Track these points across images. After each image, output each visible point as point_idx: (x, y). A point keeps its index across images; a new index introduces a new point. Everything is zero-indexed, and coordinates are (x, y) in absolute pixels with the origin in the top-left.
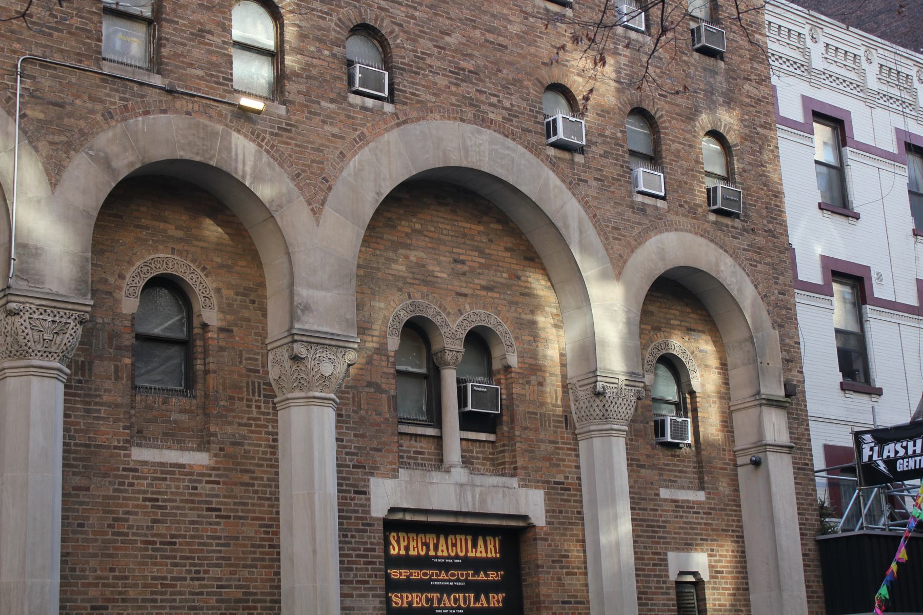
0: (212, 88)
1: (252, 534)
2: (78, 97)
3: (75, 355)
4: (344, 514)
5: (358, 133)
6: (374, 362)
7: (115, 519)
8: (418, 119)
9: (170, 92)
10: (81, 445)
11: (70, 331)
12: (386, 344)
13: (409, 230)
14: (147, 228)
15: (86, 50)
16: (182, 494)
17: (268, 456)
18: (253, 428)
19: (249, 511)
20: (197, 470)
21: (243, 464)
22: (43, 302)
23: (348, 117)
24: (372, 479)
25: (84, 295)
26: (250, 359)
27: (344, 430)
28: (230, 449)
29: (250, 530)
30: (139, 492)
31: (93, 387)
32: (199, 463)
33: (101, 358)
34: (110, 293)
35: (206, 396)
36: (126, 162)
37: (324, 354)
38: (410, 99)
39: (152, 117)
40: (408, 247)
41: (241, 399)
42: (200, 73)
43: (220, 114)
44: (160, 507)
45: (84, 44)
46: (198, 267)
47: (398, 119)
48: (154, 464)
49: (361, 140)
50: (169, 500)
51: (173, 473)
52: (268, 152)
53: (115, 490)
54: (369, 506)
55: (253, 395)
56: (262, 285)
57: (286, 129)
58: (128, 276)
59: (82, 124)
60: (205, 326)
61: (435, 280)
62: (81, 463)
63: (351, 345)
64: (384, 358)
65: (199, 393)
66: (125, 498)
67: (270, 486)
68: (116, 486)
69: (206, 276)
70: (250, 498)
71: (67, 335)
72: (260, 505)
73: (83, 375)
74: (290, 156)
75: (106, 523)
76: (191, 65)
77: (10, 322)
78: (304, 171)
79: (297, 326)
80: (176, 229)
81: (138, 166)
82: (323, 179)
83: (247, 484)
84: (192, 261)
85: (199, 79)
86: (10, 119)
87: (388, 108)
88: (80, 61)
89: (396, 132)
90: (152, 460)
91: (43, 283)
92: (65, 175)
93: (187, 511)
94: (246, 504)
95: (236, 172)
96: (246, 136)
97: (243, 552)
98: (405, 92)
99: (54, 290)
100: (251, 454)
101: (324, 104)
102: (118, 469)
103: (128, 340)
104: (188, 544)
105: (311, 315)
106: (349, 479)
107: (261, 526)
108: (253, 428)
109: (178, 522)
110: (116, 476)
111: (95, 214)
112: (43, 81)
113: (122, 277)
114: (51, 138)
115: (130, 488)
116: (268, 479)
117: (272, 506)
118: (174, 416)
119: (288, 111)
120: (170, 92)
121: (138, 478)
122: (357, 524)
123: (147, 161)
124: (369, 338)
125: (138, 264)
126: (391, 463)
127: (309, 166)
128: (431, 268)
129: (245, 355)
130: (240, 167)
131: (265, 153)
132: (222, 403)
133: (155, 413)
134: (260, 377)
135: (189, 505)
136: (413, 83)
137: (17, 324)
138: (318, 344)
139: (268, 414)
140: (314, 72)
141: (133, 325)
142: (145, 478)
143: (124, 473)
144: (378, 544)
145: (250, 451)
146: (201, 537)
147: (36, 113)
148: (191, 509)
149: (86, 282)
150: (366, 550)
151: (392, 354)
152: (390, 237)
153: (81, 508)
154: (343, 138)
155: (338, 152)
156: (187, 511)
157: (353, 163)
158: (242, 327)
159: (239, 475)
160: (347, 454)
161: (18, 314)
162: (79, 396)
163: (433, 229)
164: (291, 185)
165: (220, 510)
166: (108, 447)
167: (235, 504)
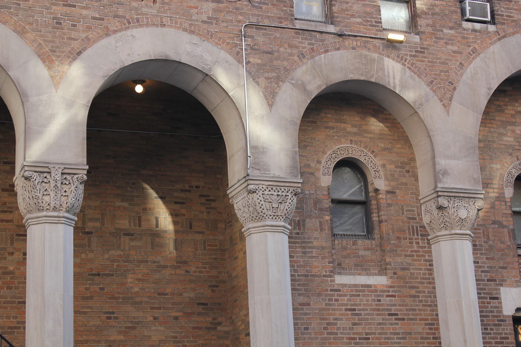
0: (368, 29)
1: (421, 330)
2: (281, 46)
3: (293, 217)
4: (484, 314)
5: (471, 48)
6: (496, 207)
7: (328, 324)
8: (514, 34)
9: (340, 35)
10: (302, 275)
12: (504, 193)
13: (514, 112)
14: (333, 128)
15: (284, 15)
16: (371, 305)
17: (427, 276)
18: (415, 257)
19: (417, 315)
20: (379, 288)
21: (410, 282)
22: (271, 183)
23: (464, 38)
24: (502, 289)
25: (296, 176)
26: (409, 210)
27: (479, 256)
28: (400, 273)
29: (419, 328)
30: (342, 305)
31: (307, 236)
32: (380, 284)
33: (310, 217)
34: (312, 174)
35: (382, 238)
36: (315, 85)
37: (460, 204)
38: (506, 20)
39: (330, 53)
40: (514, 124)
41: (405, 239)
42: (359, 20)
43: (375, 47)
44: (357, 315)
45: (282, 11)
46: (369, 151)
47: (499, 35)
48: (350, 286)
49: (474, 53)
51: (364, 291)
52: (409, 68)
53: (327, 305)
54: (501, 307)
55: (413, 235)
56: (413, 159)
57: (421, 51)
58: (323, 161)
59: (285, 63)
60: (376, 190)
62: (303, 288)
63: (479, 196)
64: (503, 203)
65: (377, 236)
66: (333, 310)
67: (430, 297)
68: (327, 302)
69: (375, 156)
71: (287, 204)
72: (424, 310)
73: (299, 229)
74: (425, 69)
75: (322, 327)
76: (353, 16)
77: (250, 198)
78: (436, 79)
79: (439, 185)
80: (352, 127)
81: (324, 87)
82: (449, 83)
83: (414, 296)
84: (364, 148)
85: (360, 25)
86: (240, 66)
87: (491, 28)
88: (281, 22)
89: (498, 44)
90: (349, 283)
91: (269, 171)
92: (278, 98)
93: (375, 316)
94: (414, 310)
95: (389, 85)
96: (394, 59)
97: (416, 343)
98: (502, 15)
100: (415, 276)
101: (445, 31)
102: (327, 290)
103: (327, 204)
104: (377, 339)
105: (449, 177)
106: (485, 289)
107: (426, 324)
109: (370, 324)
110: (326, 295)
111: (299, 122)
112: (259, 38)
113: (319, 162)
114: (266, 75)
115: (336, 303)
116: (429, 292)
117: (433, 311)
118: (361, 253)
119: (421, 39)
120: (340, 35)
121: (340, 296)
122: (494, 321)
123: (329, 84)
124: (491, 190)
125: (329, 152)
126: (514, 277)
127: (439, 75)
129: (405, 208)
130: (391, 80)
131: (407, 70)
132: (393, 242)
134: (417, 223)
135: (376, 312)
136: (508, 8)
137: (255, 199)
138: (455, 197)
139: (425, 247)
140: (437, 10)
141: (329, 194)
143: (331, 293)
144: (510, 334)
145: (414, 273)
146: (386, 334)
147: (256, 60)
148: (378, 315)
149: (297, 168)
150: (501, 338)
151: (509, 200)
152: (500, 118)
153: (305, 317)
154: (461, 53)
155: (458, 63)
156: (375, 316)
157: (470, 70)
159: (408, 290)
160: (482, 272)
161: (255, 192)
162: (298, 243)
164: (428, 89)
165: (397, 315)
166: (319, 276)
167: (407, 310)
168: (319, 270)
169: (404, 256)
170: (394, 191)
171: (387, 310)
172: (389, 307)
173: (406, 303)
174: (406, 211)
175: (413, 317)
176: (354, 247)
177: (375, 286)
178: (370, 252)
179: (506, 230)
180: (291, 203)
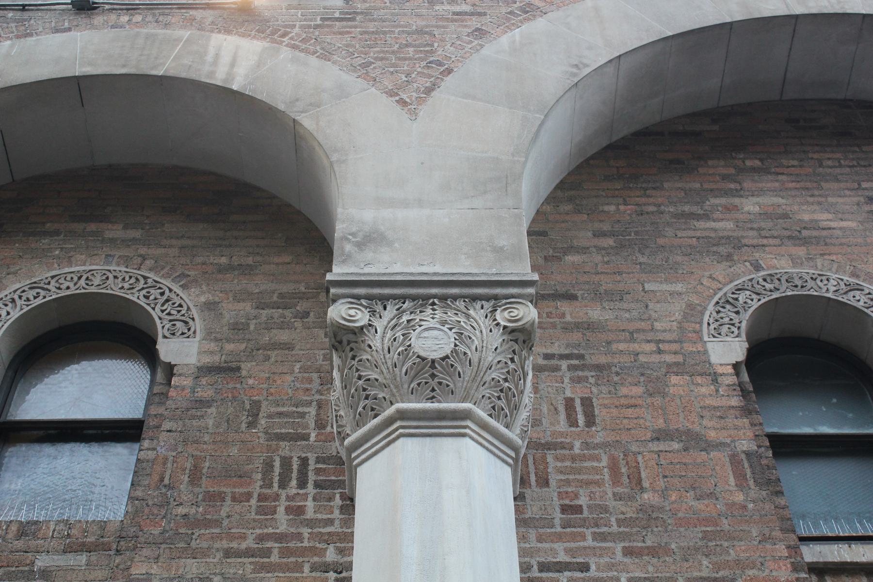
12: (706, 352)
18: (275, 558)
26: (280, 414)
27: (589, 542)
46: (166, 276)
55: (283, 485)
61: (825, 233)
108: (275, 558)
128: (806, 217)
132: (181, 510)
134: (311, 448)
138: (403, 298)
139: (331, 522)
158: (267, 358)
163: (795, 163)
169: (219, 555)
170: (234, 365)
174: (270, 416)
176: (19, 544)
179: (721, 457)
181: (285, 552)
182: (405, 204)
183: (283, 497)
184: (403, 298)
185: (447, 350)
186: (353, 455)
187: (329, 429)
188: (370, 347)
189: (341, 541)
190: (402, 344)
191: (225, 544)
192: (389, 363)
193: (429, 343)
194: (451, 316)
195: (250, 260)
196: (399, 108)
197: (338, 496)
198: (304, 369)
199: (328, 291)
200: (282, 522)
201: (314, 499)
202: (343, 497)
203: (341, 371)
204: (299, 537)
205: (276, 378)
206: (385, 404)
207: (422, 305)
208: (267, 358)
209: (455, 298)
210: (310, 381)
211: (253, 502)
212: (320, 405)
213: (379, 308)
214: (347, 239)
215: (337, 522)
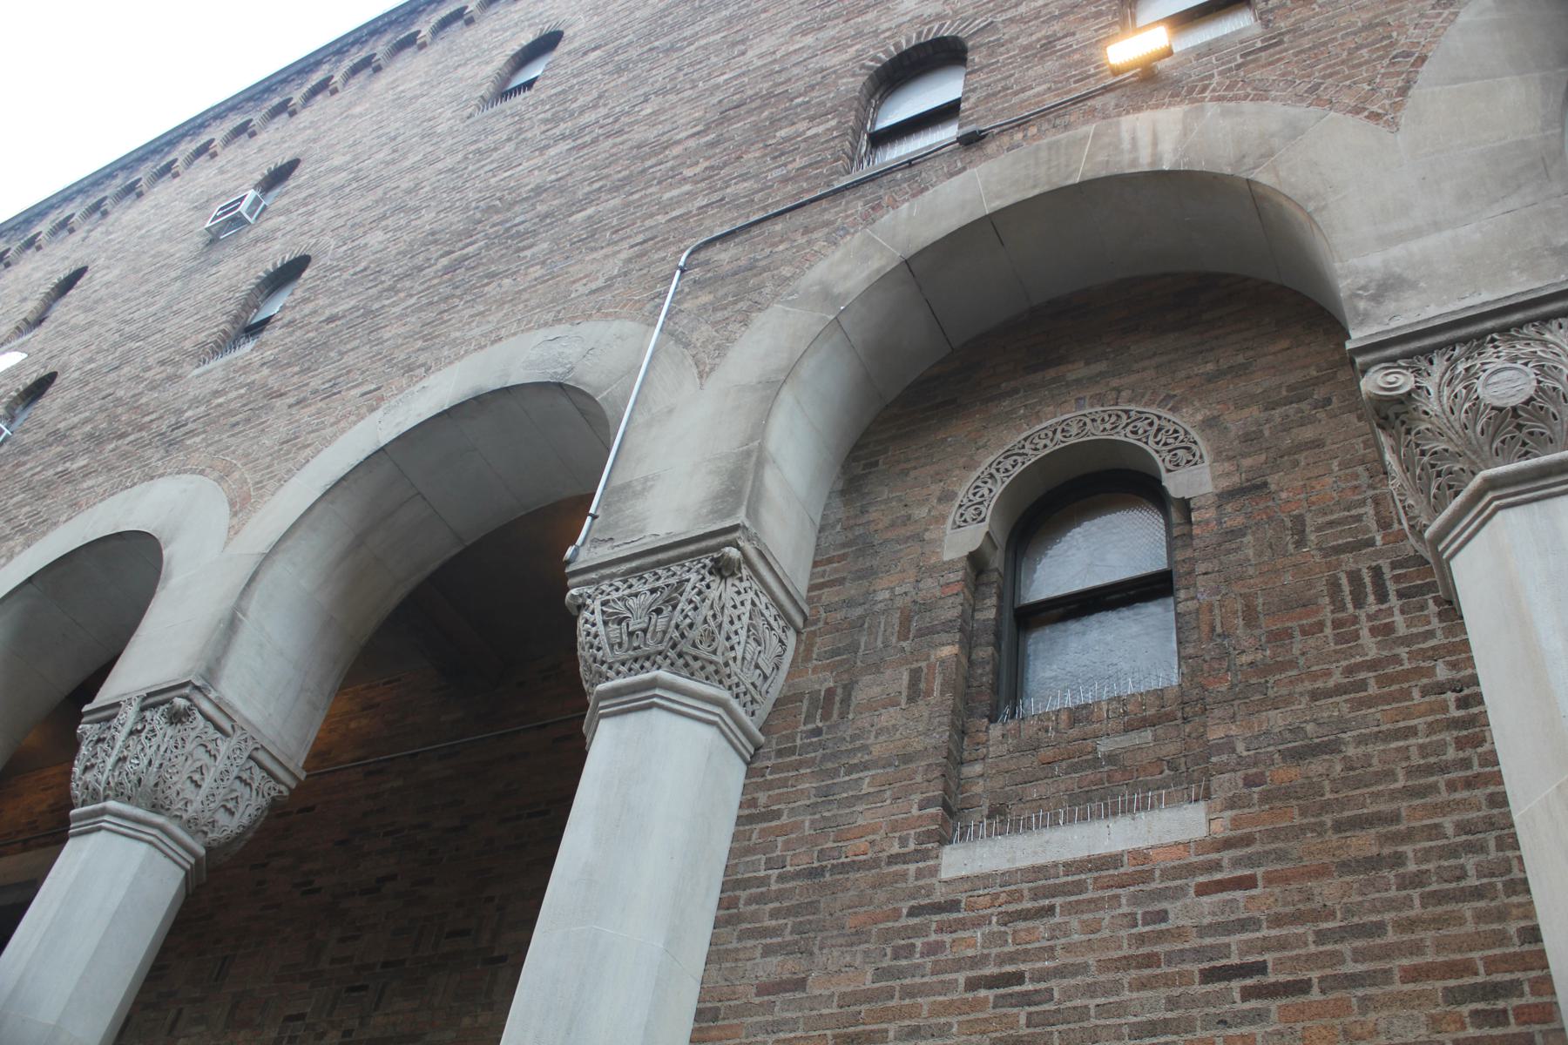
10: (797, 875)
11: (689, 592)
17: (1451, 754)
18: (1373, 689)
19: (1387, 952)
20: (1163, 861)
26: (1331, 524)
28: (1284, 774)
30: (958, 964)
32: (1168, 839)
33: (876, 668)
44: (1026, 999)
48: (1007, 878)
50: (1060, 972)
51: (1080, 887)
53: (881, 974)
58: (963, 493)
62: (790, 922)
66: (908, 992)
69: (1173, 410)
70: (1390, 905)
73: (824, 718)
83: (1372, 863)
90: (1005, 866)
93: (1127, 995)
99: (662, 532)
100: (1376, 765)
102: (896, 914)
107: (1453, 996)
108: (1373, 689)
110: (886, 936)
116: (1462, 828)
117: (1502, 915)
118: (1104, 747)
121: (951, 928)
132: (1245, 659)
133: (1046, 753)
134: (1380, 554)
135: (1134, 973)
138: (1452, 344)
142: (977, 923)
148: (1142, 985)
156: (1127, 995)
158: (1296, 464)
159: (1333, 838)
165: (1261, 968)
166: (875, 863)
167: (1321, 937)
168: (872, 843)
169: (1305, 700)
170: (1258, 481)
171: (1199, 953)
172: (1208, 941)
173: (1316, 904)
174: (1319, 529)
175: (1360, 968)
176: (1074, 732)
177: (1139, 856)
178: (1148, 734)
180: (697, 599)
181: (1383, 681)
182: (1418, 233)
183: (1363, 618)
184: (1452, 344)
185: (1530, 390)
186: (1440, 548)
187: (1396, 526)
188: (1426, 413)
189: (1450, 653)
190: (1467, 399)
191: (1308, 685)
192: (1457, 426)
193: (1501, 389)
194: (1521, 348)
195: (1240, 359)
196: (1372, 124)
197: (1431, 602)
198: (1344, 465)
199: (1353, 363)
200: (1371, 647)
201: (1402, 612)
202: (1437, 601)
203: (1396, 451)
204: (1396, 659)
205: (1314, 483)
206: (1464, 477)
207: (1478, 346)
208: (1296, 464)
209: (1520, 325)
210: (1356, 476)
211: (1328, 631)
212: (1377, 502)
213: (1423, 364)
214: (1360, 296)
215: (1439, 633)
